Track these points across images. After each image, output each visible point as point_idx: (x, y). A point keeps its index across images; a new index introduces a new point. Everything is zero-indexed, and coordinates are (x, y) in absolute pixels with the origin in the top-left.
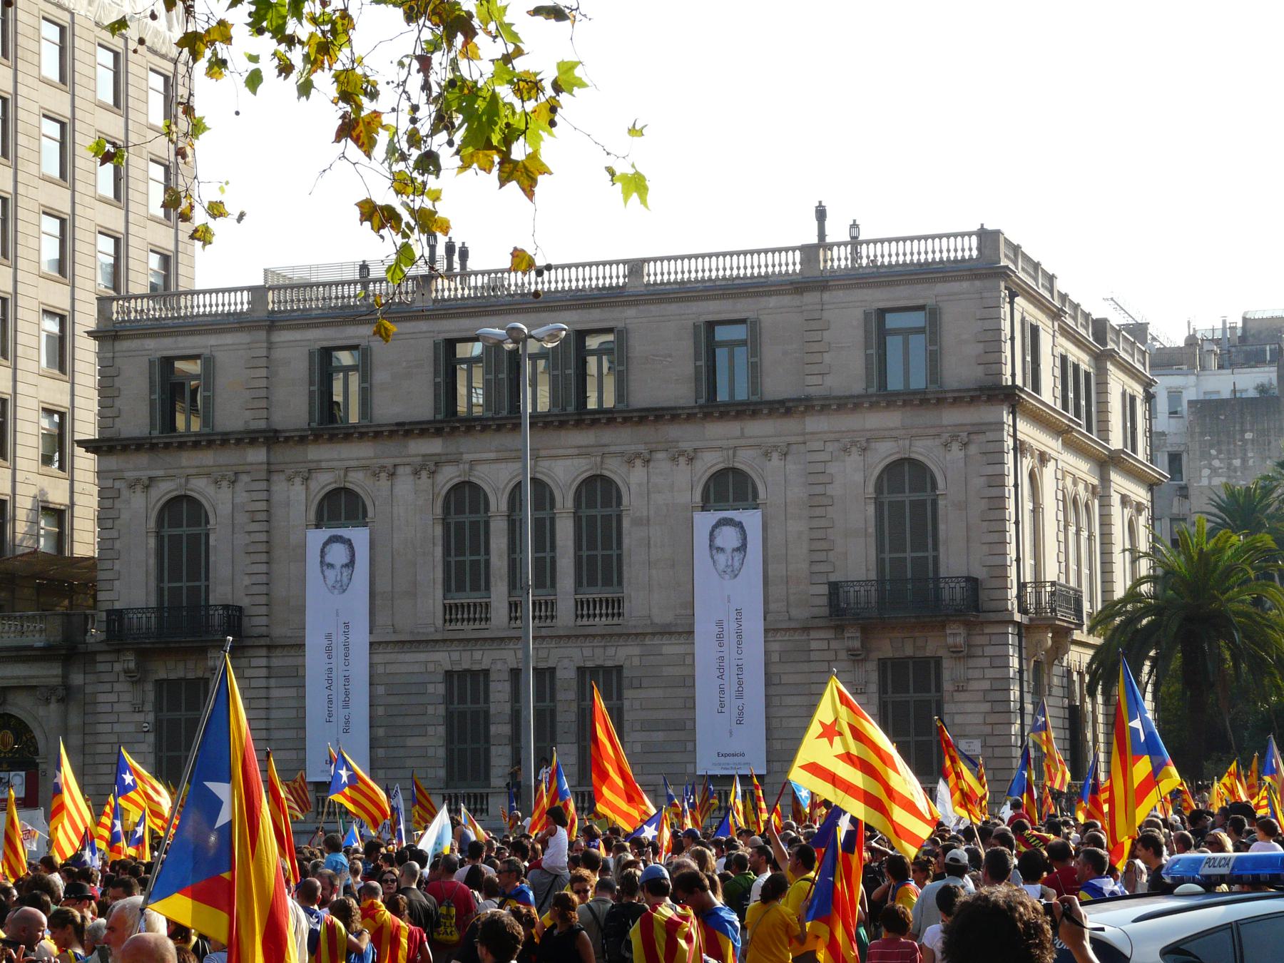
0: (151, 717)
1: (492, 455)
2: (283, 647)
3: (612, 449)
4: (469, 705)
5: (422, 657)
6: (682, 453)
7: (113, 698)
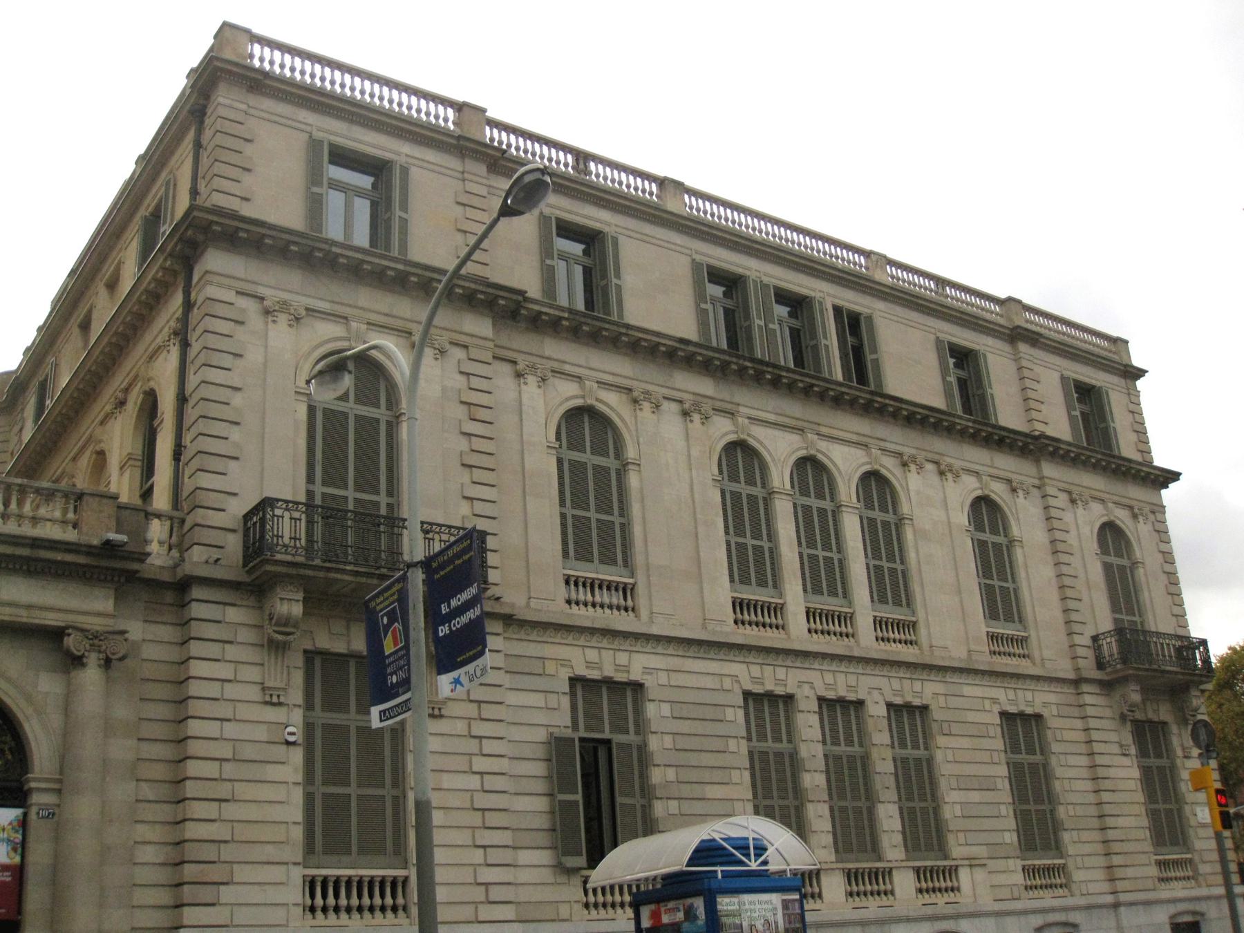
0: (297, 716)
1: (772, 417)
2: (523, 624)
3: (888, 446)
4: (770, 743)
5: (714, 667)
6: (950, 468)
7: (224, 671)
